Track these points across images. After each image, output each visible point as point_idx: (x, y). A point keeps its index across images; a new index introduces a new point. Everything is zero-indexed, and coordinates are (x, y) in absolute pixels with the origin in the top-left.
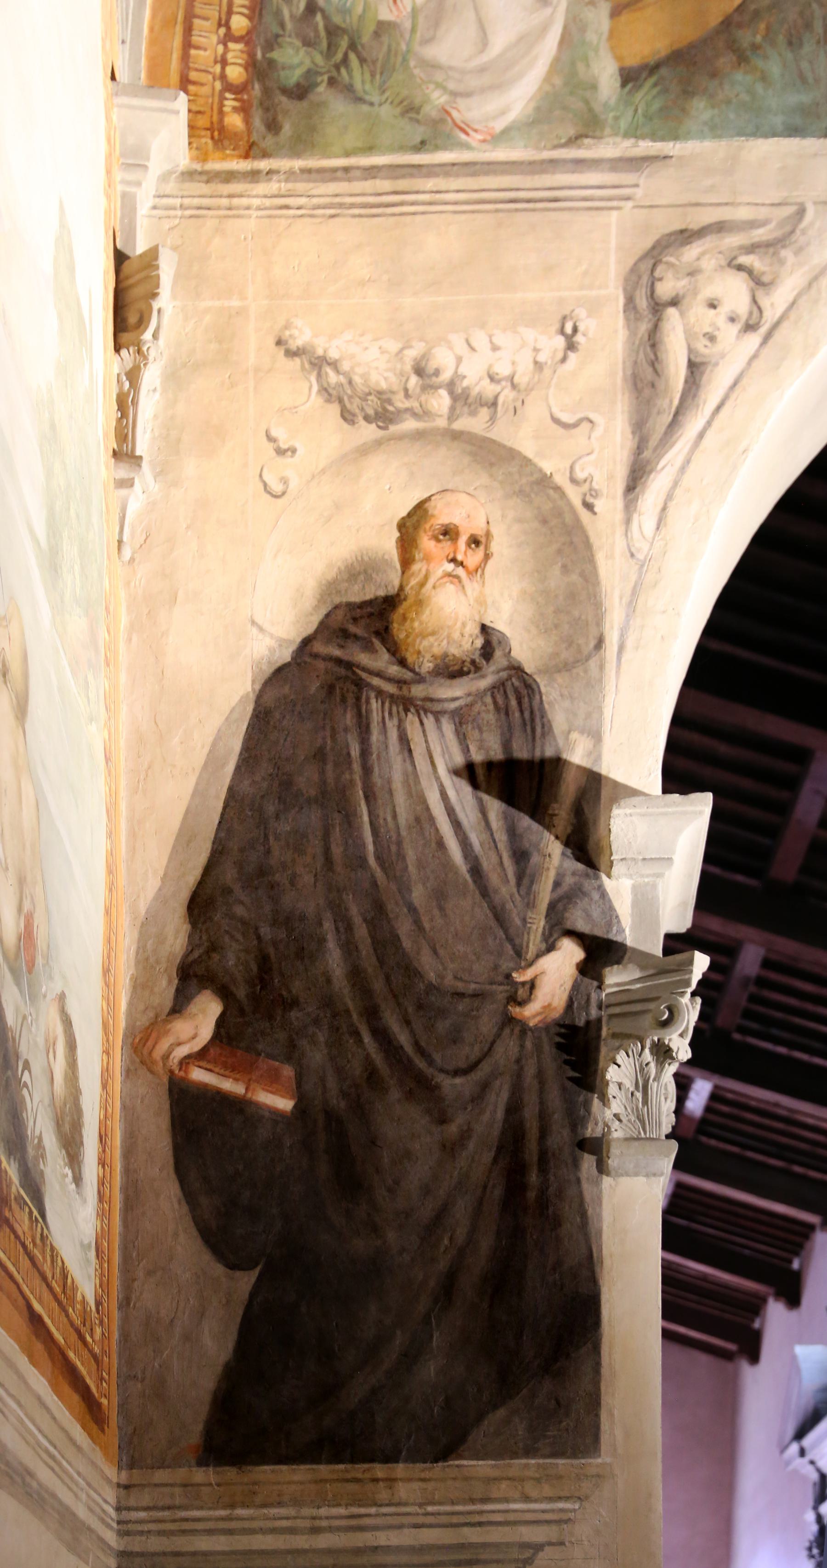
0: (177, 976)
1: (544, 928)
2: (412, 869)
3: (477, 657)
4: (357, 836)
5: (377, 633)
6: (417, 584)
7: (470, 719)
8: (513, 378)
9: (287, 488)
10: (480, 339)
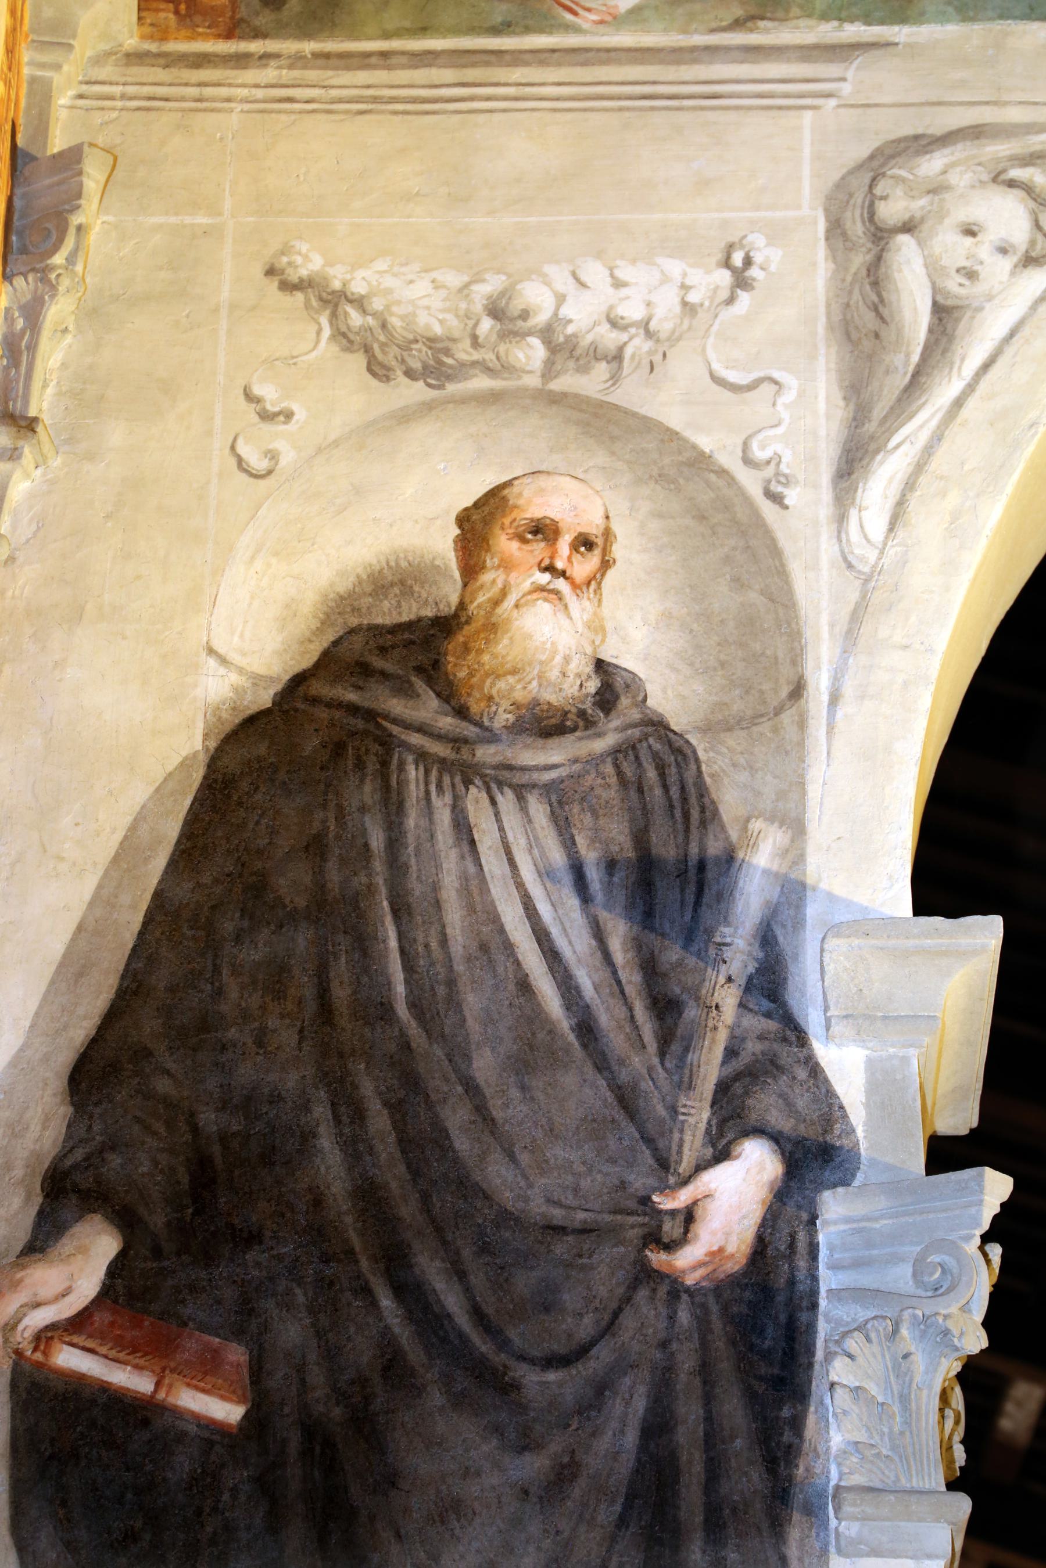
0: (43, 1191)
1: (709, 1123)
2: (473, 1025)
3: (588, 706)
4: (376, 970)
5: (419, 670)
6: (489, 600)
7: (577, 796)
8: (647, 323)
9: (276, 464)
10: (595, 272)
